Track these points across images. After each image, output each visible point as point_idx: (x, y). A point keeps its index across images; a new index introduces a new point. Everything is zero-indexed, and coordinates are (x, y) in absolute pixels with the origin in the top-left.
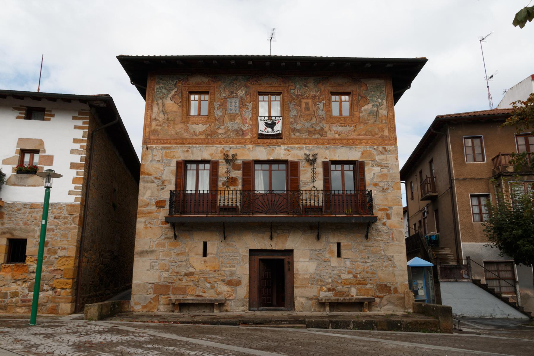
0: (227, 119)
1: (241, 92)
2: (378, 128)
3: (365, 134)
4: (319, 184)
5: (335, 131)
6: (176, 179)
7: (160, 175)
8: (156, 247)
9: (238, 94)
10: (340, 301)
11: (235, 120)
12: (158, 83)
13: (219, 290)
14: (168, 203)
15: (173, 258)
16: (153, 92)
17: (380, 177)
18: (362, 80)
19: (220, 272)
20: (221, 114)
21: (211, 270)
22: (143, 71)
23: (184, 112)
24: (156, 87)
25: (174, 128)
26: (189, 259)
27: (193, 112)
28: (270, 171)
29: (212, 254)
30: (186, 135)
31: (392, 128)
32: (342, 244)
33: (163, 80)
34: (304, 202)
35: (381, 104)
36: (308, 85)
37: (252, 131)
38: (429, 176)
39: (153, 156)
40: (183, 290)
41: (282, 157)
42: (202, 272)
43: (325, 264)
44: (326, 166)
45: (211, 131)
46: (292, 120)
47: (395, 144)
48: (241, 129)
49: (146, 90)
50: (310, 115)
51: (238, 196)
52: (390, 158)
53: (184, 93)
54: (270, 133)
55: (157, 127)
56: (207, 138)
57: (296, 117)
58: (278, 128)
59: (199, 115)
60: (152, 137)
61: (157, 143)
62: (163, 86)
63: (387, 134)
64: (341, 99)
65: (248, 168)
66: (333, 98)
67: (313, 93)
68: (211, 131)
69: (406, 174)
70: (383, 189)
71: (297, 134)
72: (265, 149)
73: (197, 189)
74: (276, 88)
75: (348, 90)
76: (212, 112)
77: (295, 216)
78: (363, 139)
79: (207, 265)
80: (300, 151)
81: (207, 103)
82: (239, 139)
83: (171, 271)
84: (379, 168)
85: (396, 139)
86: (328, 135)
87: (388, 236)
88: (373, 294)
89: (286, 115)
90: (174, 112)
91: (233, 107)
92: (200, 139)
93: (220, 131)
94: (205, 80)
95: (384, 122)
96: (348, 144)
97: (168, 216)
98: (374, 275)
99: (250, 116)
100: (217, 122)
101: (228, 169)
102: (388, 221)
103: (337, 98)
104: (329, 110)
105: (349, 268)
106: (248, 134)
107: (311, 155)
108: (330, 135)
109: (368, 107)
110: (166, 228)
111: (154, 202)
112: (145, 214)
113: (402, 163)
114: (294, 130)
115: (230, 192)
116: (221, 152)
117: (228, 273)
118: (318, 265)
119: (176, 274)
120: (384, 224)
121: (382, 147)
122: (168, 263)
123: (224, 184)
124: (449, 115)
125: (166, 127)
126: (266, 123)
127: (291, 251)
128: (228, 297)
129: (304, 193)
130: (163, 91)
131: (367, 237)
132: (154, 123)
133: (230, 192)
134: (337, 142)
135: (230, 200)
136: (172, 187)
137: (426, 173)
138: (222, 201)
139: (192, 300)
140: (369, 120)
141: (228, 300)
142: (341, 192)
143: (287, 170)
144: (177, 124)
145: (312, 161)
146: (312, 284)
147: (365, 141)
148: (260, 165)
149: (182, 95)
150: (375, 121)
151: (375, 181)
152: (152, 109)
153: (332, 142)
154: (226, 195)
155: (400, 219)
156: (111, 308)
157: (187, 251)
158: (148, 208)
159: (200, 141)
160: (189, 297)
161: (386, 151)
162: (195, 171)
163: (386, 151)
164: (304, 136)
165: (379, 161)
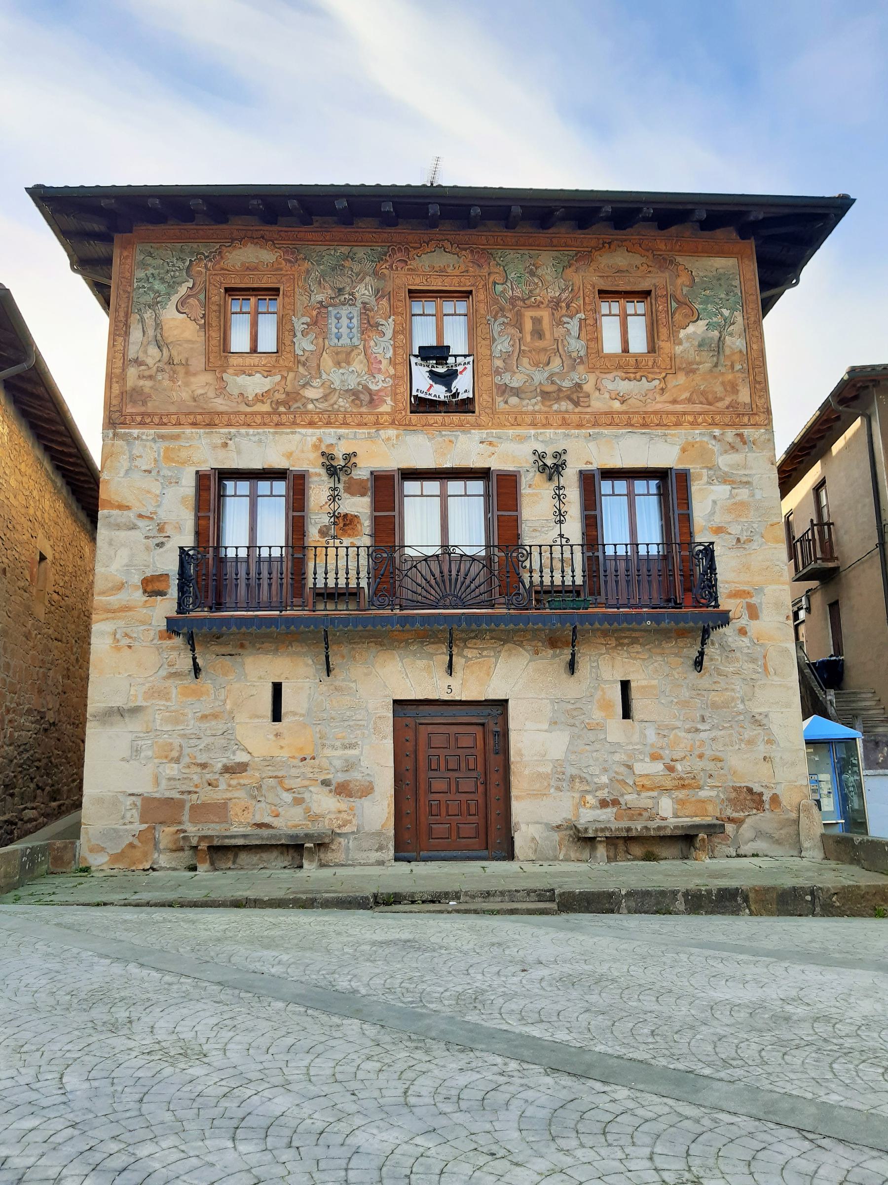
0: (327, 361)
1: (364, 291)
2: (723, 383)
3: (690, 400)
4: (574, 529)
5: (608, 391)
6: (198, 518)
7: (151, 509)
8: (145, 699)
10: (634, 834)
11: (348, 363)
13: (316, 809)
14: (174, 582)
15: (192, 725)
17: (729, 511)
18: (679, 259)
19: (317, 761)
20: (312, 347)
21: (293, 757)
22: (97, 225)
23: (214, 342)
25: (187, 384)
26: (233, 728)
27: (239, 341)
28: (444, 497)
29: (295, 714)
30: (220, 404)
31: (759, 383)
32: (633, 684)
39: (132, 458)
40: (221, 810)
42: (270, 761)
43: (591, 736)
44: (589, 482)
45: (288, 394)
46: (499, 363)
47: (768, 423)
48: (366, 388)
50: (545, 350)
51: (363, 561)
53: (213, 291)
55: (141, 383)
56: (275, 412)
57: (509, 355)
59: (254, 350)
60: (130, 409)
61: (142, 424)
62: (156, 272)
63: (747, 400)
65: (386, 489)
68: (288, 394)
70: (738, 540)
71: (514, 400)
72: (430, 439)
74: (456, 280)
76: (287, 342)
78: (684, 413)
79: (282, 743)
82: (361, 414)
83: (186, 760)
84: (729, 487)
85: (768, 412)
86: (593, 403)
87: (754, 660)
88: (718, 815)
89: (483, 351)
90: (188, 341)
91: (344, 330)
94: (266, 256)
95: (738, 367)
96: (645, 425)
97: (175, 614)
98: (719, 764)
99: (390, 354)
100: (301, 369)
102: (754, 623)
105: (652, 745)
106: (385, 401)
108: (598, 403)
109: (697, 329)
110: (173, 648)
111: (137, 579)
114: (504, 390)
116: (316, 447)
117: (338, 763)
118: (572, 737)
119: (199, 770)
120: (743, 632)
121: (735, 431)
122: (177, 741)
123: (323, 532)
125: (166, 383)
126: (431, 372)
127: (503, 704)
128: (339, 827)
131: (698, 664)
134: (617, 421)
136: (188, 540)
139: (245, 836)
141: (339, 835)
143: (487, 495)
144: (195, 374)
145: (552, 469)
146: (558, 789)
148: (418, 483)
150: (716, 365)
151: (718, 520)
152: (127, 334)
155: (783, 619)
156: (23, 865)
157: (228, 707)
160: (235, 830)
161: (745, 443)
163: (745, 443)
164: (533, 405)
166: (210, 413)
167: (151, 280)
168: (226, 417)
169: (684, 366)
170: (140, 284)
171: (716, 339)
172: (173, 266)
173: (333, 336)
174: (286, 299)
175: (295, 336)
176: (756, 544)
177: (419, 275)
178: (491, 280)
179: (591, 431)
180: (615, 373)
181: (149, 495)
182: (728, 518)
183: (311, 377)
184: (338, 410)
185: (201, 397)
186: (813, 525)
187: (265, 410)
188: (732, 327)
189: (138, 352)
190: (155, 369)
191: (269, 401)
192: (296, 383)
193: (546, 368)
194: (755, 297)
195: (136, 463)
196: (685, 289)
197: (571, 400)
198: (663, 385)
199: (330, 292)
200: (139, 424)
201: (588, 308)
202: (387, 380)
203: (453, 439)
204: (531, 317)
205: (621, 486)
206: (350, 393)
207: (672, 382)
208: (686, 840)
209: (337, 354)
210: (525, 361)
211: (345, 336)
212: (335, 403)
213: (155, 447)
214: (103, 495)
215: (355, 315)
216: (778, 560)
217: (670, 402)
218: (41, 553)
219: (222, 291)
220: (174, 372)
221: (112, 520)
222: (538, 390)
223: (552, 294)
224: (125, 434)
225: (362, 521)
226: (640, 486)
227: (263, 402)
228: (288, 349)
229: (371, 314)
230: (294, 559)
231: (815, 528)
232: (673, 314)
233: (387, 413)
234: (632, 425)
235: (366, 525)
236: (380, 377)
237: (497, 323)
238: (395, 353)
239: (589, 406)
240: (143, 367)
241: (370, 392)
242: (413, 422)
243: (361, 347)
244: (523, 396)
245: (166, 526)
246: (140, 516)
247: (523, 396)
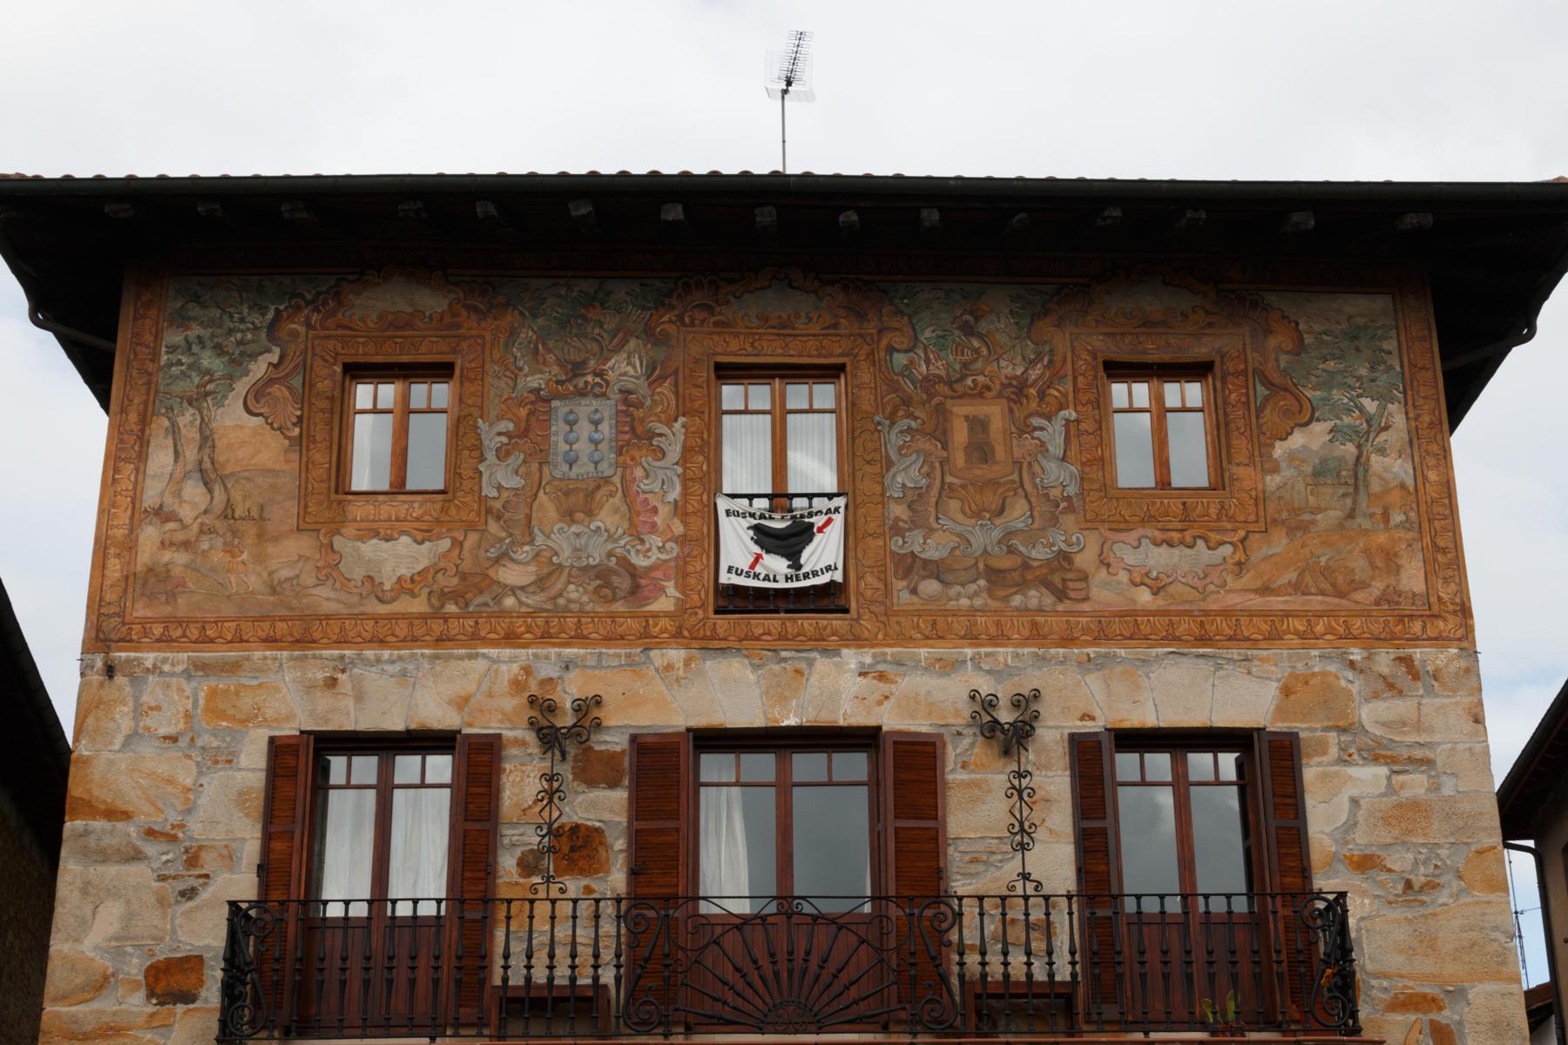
0: (547, 506)
1: (625, 368)
2: (1367, 552)
3: (1297, 588)
4: (1055, 862)
6: (268, 837)
7: (174, 818)
9: (611, 376)
11: (590, 514)
12: (181, 320)
14: (215, 975)
16: (150, 367)
17: (1386, 820)
18: (1271, 298)
20: (516, 482)
23: (318, 473)
25: (260, 559)
27: (367, 472)
28: (784, 787)
30: (325, 599)
31: (1444, 551)
33: (204, 306)
34: (972, 959)
35: (1375, 425)
36: (983, 327)
37: (682, 575)
39: (139, 712)
41: (848, 714)
44: (1090, 758)
45: (464, 577)
46: (898, 511)
47: (1468, 632)
48: (624, 562)
49: (111, 356)
50: (994, 483)
51: (608, 927)
52: (1440, 712)
54: (782, 585)
55: (167, 556)
56: (438, 614)
58: (824, 555)
59: (399, 487)
60: (141, 611)
61: (165, 641)
62: (205, 333)
63: (1418, 586)
64: (1158, 398)
65: (663, 773)
67: (1011, 368)
68: (464, 577)
70: (1409, 885)
71: (930, 587)
72: (756, 667)
73: (380, 895)
74: (812, 344)
75: (1200, 351)
77: (920, 1039)
78: (1287, 614)
80: (944, 682)
81: (440, 423)
82: (613, 616)
84: (1383, 771)
85: (1465, 611)
86: (1095, 592)
90: (266, 472)
91: (583, 447)
93: (511, 575)
94: (432, 302)
95: (1397, 518)
96: (1203, 640)
99: (675, 494)
100: (493, 527)
106: (663, 590)
107: (1004, 702)
108: (1106, 592)
109: (1309, 440)
111: (135, 967)
114: (910, 566)
115: (565, 908)
116: (517, 686)
121: (1393, 653)
123: (528, 865)
125: (218, 557)
126: (757, 529)
129: (970, 910)
130: (205, 363)
132: (150, 535)
133: (565, 908)
134: (1146, 629)
135: (562, 953)
136: (243, 885)
138: (517, 961)
140: (1318, 510)
142: (1174, 906)
143: (874, 784)
144: (276, 539)
145: (1009, 734)
147: (1299, 625)
148: (730, 758)
149: (308, 384)
150: (1351, 515)
151: (1362, 840)
152: (142, 457)
154: (541, 926)
158: (105, 1006)
159: (402, 629)
161: (1416, 677)
162: (371, 795)
164: (968, 596)
165: (1378, 731)
166: (302, 618)
167: (195, 349)
168: (335, 626)
169: (1284, 515)
170: (174, 358)
171: (1351, 460)
172: (242, 320)
173: (560, 459)
174: (467, 384)
175: (482, 459)
176: (1446, 892)
177: (736, 335)
178: (884, 343)
179: (1091, 651)
180: (1140, 532)
181: (170, 789)
183: (512, 543)
184: (567, 610)
185: (286, 586)
187: (415, 610)
188: (1383, 436)
189: (162, 494)
190: (195, 528)
191: (426, 590)
192: (482, 554)
193: (997, 521)
194: (1430, 374)
195: (148, 721)
197: (1049, 585)
199: (556, 369)
200: (158, 641)
201: (1084, 398)
202: (669, 545)
203: (803, 666)
204: (967, 417)
206: (592, 573)
209: (567, 494)
211: (584, 459)
212: (560, 595)
213: (188, 688)
215: (606, 415)
216: (1496, 928)
217: (1256, 591)
219: (338, 369)
220: (234, 534)
221: (92, 841)
222: (981, 566)
223: (1009, 371)
224: (129, 661)
225: (609, 840)
227: (413, 595)
228: (467, 485)
229: (639, 413)
232: (1260, 410)
233: (667, 615)
234: (1178, 639)
237: (896, 429)
238: (685, 493)
239: (1086, 599)
240: (171, 525)
241: (633, 572)
242: (721, 632)
243: (617, 480)
244: (950, 578)
245: (203, 854)
246: (151, 833)
247: (950, 578)
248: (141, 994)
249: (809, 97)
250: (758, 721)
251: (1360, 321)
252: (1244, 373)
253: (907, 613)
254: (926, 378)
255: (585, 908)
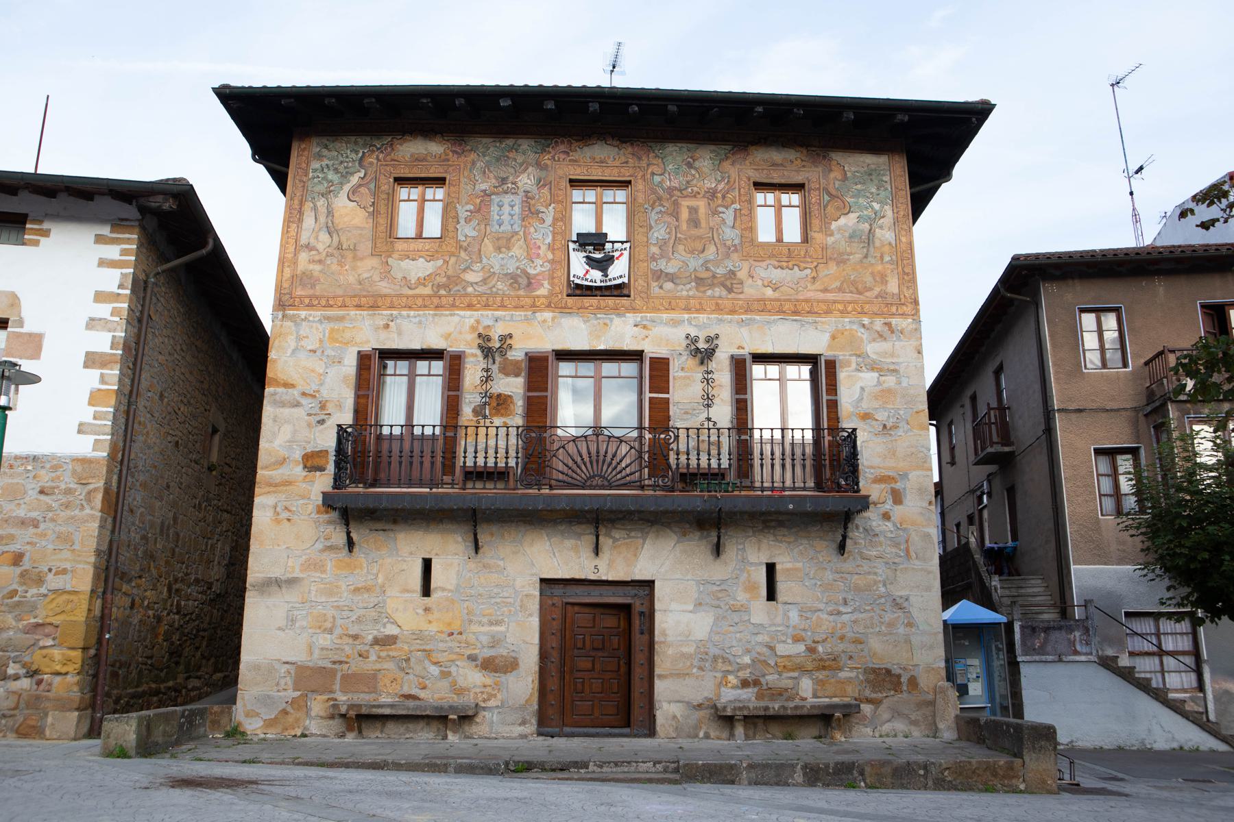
0: (488, 245)
1: (526, 180)
2: (872, 273)
3: (840, 290)
4: (723, 413)
5: (761, 280)
7: (314, 387)
8: (301, 571)
9: (520, 184)
10: (771, 712)
11: (509, 249)
12: (319, 157)
13: (461, 682)
14: (332, 459)
16: (305, 179)
17: (876, 398)
19: (464, 637)
20: (474, 234)
21: (442, 632)
22: (277, 123)
23: (382, 228)
24: (310, 160)
25: (354, 268)
26: (384, 602)
28: (598, 379)
29: (443, 589)
30: (384, 287)
31: (908, 274)
32: (778, 567)
33: (329, 150)
34: (683, 458)
35: (878, 215)
36: (697, 164)
37: (552, 278)
38: (994, 404)
39: (299, 338)
40: (370, 681)
41: (628, 345)
42: (419, 635)
43: (736, 617)
45: (449, 278)
46: (654, 250)
47: (916, 313)
48: (525, 272)
49: (286, 175)
50: (700, 238)
51: (513, 440)
52: (902, 349)
53: (383, 180)
54: (598, 284)
55: (311, 267)
57: (665, 242)
58: (619, 270)
59: (419, 236)
60: (299, 292)
61: (310, 306)
63: (896, 291)
64: (779, 201)
65: (539, 370)
66: (760, 197)
67: (710, 184)
68: (449, 278)
69: (944, 396)
70: (885, 426)
71: (669, 286)
72: (585, 322)
73: (410, 425)
74: (616, 171)
75: (798, 178)
76: (451, 228)
78: (835, 302)
79: (430, 617)
80: (675, 330)
81: (439, 206)
82: (518, 297)
83: (338, 631)
84: (876, 375)
86: (746, 290)
87: (897, 545)
88: (857, 695)
89: (640, 238)
91: (506, 217)
92: (420, 296)
93: (471, 277)
94: (435, 148)
95: (887, 258)
96: (796, 313)
98: (860, 647)
99: (549, 240)
100: (463, 254)
101: (487, 370)
102: (898, 508)
103: (770, 197)
104: (750, 228)
105: (794, 627)
108: (751, 290)
109: (848, 221)
111: (298, 455)
112: (276, 485)
113: (931, 374)
114: (659, 275)
115: (492, 431)
116: (473, 328)
117: (485, 639)
118: (717, 619)
119: (351, 641)
120: (886, 516)
122: (331, 612)
124: (1044, 255)
125: (335, 267)
126: (587, 257)
127: (650, 584)
128: (484, 701)
129: (682, 434)
131: (842, 548)
132: (303, 256)
133: (492, 431)
134: (769, 307)
135: (491, 452)
136: (347, 418)
137: (987, 397)
138: (470, 455)
140: (851, 254)
141: (484, 709)
142: (777, 435)
144: (361, 259)
145: (704, 354)
146: (701, 668)
147: (840, 307)
149: (377, 187)
150: (866, 257)
151: (865, 406)
152: (300, 220)
153: (756, 306)
154: (482, 439)
155: (925, 504)
157: (380, 581)
159: (419, 302)
160: (384, 699)
161: (893, 332)
163: (893, 332)
164: (686, 290)
165: (874, 357)
168: (389, 300)
171: (867, 231)
175: (458, 222)
179: (744, 317)
182: (876, 404)
186: (990, 409)
195: (302, 343)
196: (837, 183)
197: (725, 286)
198: (814, 274)
205: (773, 370)
207: (823, 271)
208: (825, 720)
209: (498, 239)
210: (681, 248)
211: (506, 223)
214: (270, 373)
218: (213, 426)
221: (277, 397)
226: (792, 370)
228: (451, 234)
229: (533, 202)
230: (446, 438)
231: (992, 412)
233: (544, 297)
235: (519, 404)
236: (539, 262)
244: (678, 281)
246: (304, 394)
247: (678, 281)
248: (301, 466)
249: (623, 73)
250: (587, 347)
251: (873, 167)
252: (819, 189)
253: (657, 298)
254: (669, 188)
255: (502, 431)
